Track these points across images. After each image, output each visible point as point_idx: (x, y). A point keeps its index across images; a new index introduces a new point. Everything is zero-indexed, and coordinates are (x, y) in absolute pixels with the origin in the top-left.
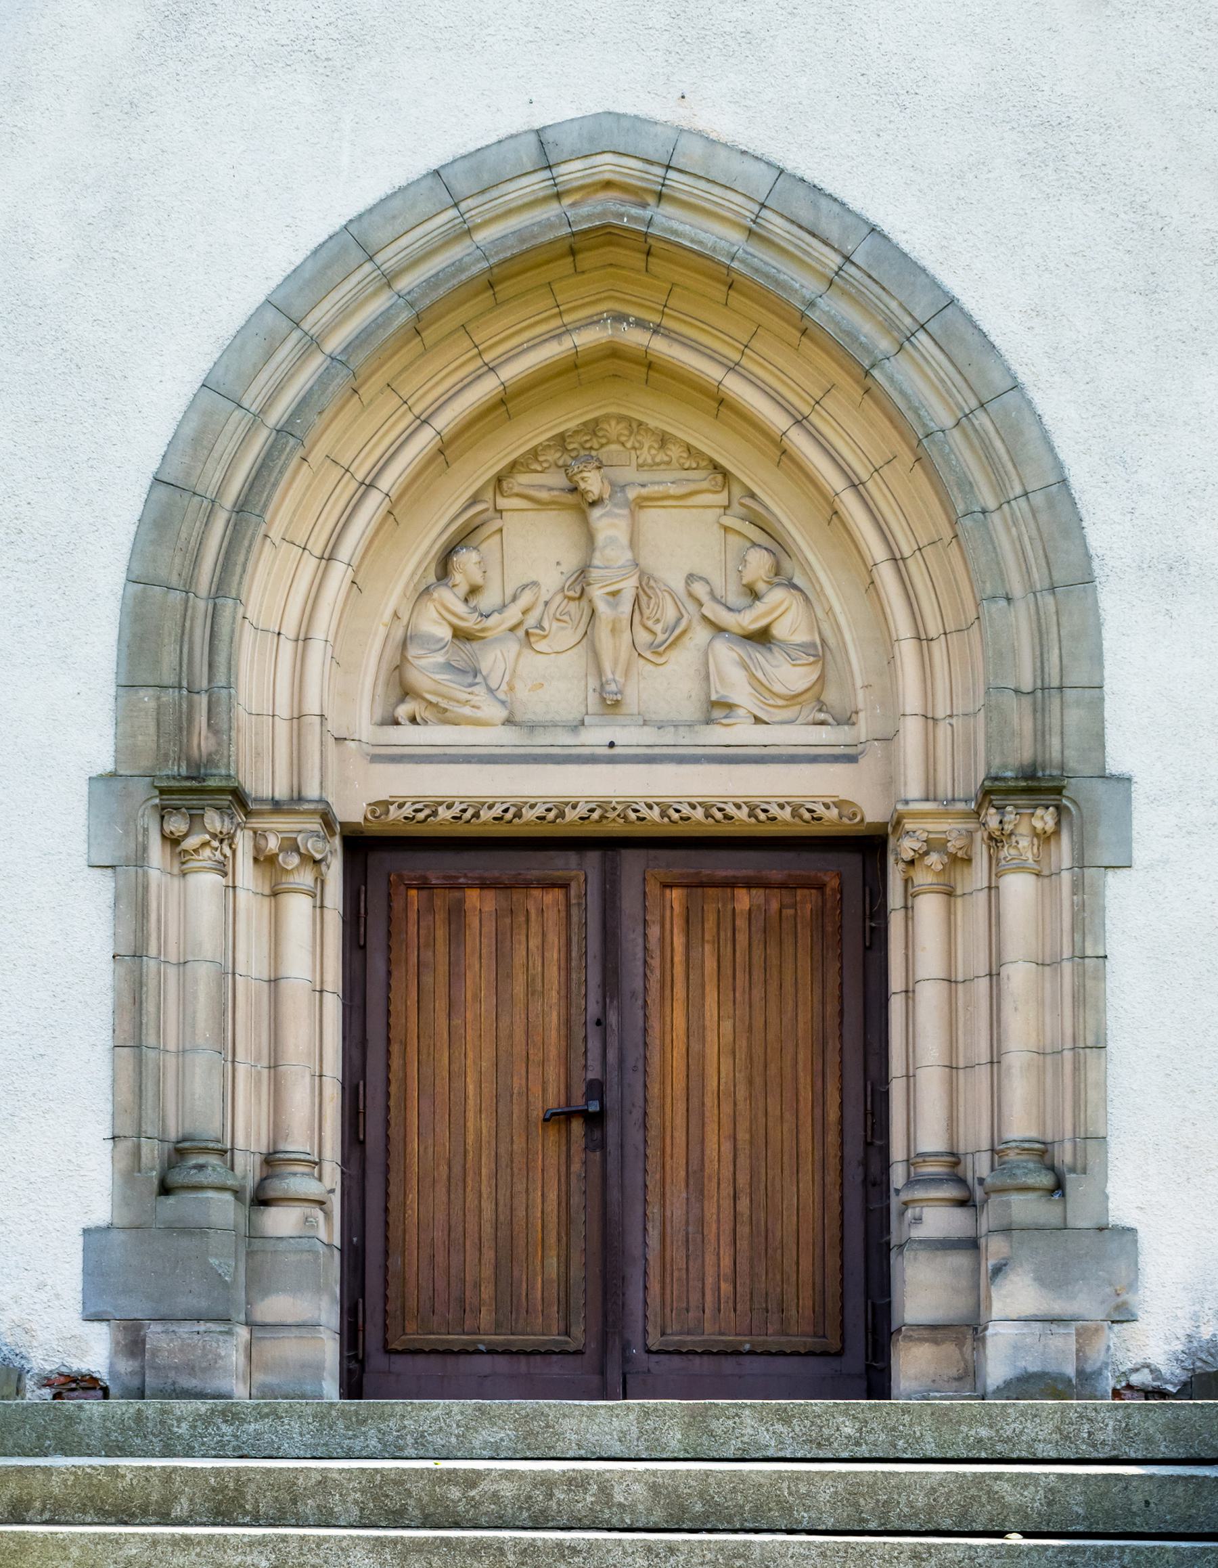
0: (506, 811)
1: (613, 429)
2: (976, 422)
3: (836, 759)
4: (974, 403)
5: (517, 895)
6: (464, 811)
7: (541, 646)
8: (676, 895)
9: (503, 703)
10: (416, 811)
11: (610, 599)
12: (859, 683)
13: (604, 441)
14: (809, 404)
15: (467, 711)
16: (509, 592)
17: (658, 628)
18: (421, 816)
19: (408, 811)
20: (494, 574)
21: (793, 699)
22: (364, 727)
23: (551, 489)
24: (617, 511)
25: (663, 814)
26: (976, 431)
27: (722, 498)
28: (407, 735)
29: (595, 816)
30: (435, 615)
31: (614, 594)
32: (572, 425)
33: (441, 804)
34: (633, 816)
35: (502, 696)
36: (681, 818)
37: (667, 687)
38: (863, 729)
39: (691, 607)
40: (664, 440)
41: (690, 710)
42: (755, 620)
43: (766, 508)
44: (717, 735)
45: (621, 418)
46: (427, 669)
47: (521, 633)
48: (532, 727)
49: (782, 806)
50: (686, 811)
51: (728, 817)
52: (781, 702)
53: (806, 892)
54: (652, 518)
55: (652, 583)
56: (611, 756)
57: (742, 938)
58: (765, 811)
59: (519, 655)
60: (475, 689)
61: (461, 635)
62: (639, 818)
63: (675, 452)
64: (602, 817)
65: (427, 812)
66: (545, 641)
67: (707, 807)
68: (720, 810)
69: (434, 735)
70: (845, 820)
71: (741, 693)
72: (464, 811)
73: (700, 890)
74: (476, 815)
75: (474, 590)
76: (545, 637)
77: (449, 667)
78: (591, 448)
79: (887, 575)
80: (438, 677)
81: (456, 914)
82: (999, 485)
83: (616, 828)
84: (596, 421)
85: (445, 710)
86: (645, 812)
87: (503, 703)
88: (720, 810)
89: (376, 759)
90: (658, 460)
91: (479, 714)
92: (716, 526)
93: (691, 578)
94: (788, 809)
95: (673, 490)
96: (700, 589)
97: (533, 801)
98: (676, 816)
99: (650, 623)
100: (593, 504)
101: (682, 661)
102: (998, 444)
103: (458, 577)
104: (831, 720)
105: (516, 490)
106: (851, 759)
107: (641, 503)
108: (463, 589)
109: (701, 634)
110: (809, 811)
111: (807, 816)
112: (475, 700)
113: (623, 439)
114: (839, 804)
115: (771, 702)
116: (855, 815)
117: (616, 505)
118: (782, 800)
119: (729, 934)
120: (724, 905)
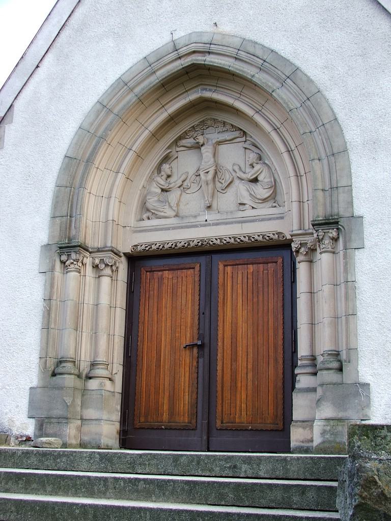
0: (172, 245)
1: (209, 123)
2: (307, 104)
3: (277, 218)
4: (305, 98)
5: (179, 272)
6: (160, 246)
7: (188, 191)
8: (229, 269)
9: (174, 210)
10: (146, 247)
11: (206, 174)
12: (285, 193)
13: (207, 127)
14: (260, 106)
15: (162, 214)
16: (179, 176)
17: (223, 182)
18: (147, 249)
19: (143, 247)
20: (174, 170)
21: (265, 200)
22: (132, 221)
23: (191, 143)
24: (208, 147)
25: (221, 242)
26: (307, 107)
27: (244, 139)
28: (147, 223)
29: (200, 244)
30: (155, 185)
31: (207, 172)
32: (196, 123)
33: (153, 244)
34: (211, 243)
35: (174, 208)
36: (227, 243)
37: (226, 201)
38: (286, 209)
39: (234, 174)
40: (224, 123)
41: (233, 207)
42: (251, 176)
43: (255, 140)
44: (241, 214)
45: (211, 119)
46: (152, 202)
47: (182, 188)
48: (182, 218)
49: (259, 236)
50: (228, 240)
51: (241, 241)
52: (260, 201)
53: (271, 264)
54: (223, 148)
55: (221, 168)
56: (206, 224)
57: (250, 281)
58: (253, 238)
59: (181, 195)
60: (165, 207)
61: (163, 190)
62: (214, 244)
63: (228, 127)
64: (202, 244)
65: (149, 247)
66: (189, 190)
67: (235, 238)
68: (239, 239)
69: (155, 222)
70: (280, 239)
71: (247, 200)
72: (160, 246)
73: (236, 266)
74: (163, 247)
75: (169, 176)
76: (189, 188)
77: (159, 201)
78: (204, 129)
79: (286, 156)
80: (154, 204)
81: (161, 279)
82: (315, 123)
83: (207, 248)
84: (203, 121)
85: (157, 214)
86: (215, 241)
87: (174, 210)
88: (239, 239)
89: (135, 232)
90: (224, 130)
91: (166, 215)
92: (242, 148)
93: (234, 164)
94: (261, 237)
95: (228, 138)
96: (236, 168)
97: (180, 241)
98: (225, 242)
99: (220, 180)
100: (202, 145)
101: (231, 191)
102: (314, 110)
103: (163, 173)
104: (277, 206)
105: (181, 145)
106: (282, 218)
107: (219, 143)
108: (165, 176)
109: (237, 182)
110: (268, 236)
111: (267, 238)
112: (165, 210)
113: (213, 125)
114: (279, 233)
115: (257, 201)
116: (284, 237)
117: (208, 145)
118: (259, 234)
119: (246, 280)
120: (244, 271)
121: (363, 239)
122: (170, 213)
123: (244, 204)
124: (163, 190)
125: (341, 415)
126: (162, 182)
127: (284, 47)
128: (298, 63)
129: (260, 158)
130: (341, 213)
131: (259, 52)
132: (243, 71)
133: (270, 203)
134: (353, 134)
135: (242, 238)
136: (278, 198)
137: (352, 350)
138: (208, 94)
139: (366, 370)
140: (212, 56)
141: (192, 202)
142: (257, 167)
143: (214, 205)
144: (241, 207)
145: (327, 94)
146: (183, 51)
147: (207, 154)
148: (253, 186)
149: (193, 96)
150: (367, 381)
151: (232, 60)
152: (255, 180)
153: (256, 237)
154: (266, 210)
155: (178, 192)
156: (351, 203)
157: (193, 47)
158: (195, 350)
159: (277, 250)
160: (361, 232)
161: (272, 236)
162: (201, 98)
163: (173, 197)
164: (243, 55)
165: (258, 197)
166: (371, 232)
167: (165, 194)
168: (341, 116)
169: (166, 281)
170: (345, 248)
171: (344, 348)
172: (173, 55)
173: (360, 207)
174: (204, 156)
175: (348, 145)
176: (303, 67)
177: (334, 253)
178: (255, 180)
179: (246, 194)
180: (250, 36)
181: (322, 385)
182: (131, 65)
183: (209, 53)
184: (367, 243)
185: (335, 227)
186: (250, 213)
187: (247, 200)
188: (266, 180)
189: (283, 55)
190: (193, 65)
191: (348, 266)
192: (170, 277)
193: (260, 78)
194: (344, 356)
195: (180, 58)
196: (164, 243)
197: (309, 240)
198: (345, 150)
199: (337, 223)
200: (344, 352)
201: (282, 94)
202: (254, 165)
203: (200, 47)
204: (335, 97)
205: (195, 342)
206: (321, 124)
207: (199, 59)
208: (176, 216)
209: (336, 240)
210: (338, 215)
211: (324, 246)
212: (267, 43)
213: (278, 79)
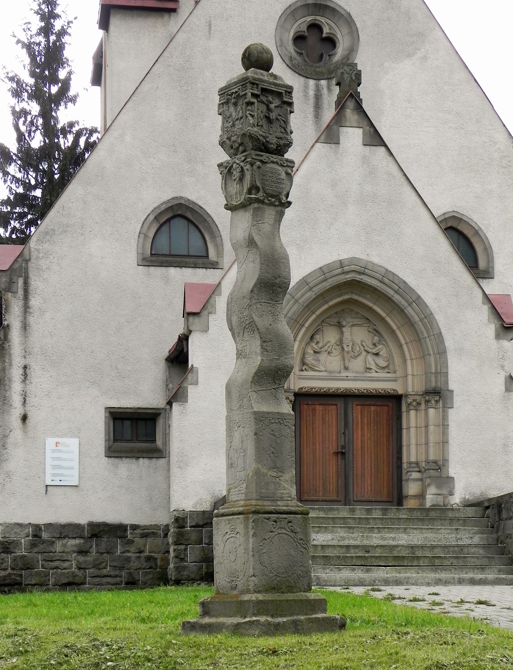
5: (327, 406)
8: (359, 407)
15: (318, 369)
17: (355, 352)
21: (383, 368)
28: (305, 373)
31: (348, 346)
39: (362, 348)
40: (357, 313)
41: (362, 369)
46: (310, 359)
48: (331, 372)
50: (363, 390)
54: (355, 328)
56: (347, 379)
57: (372, 416)
71: (373, 367)
77: (314, 359)
81: (314, 410)
83: (349, 393)
93: (362, 341)
95: (359, 323)
96: (364, 344)
103: (315, 341)
107: (353, 325)
108: (315, 343)
109: (364, 353)
114: (394, 390)
121: (452, 403)
122: (322, 368)
123: (371, 369)
124: (315, 352)
125: (439, 492)
126: (316, 347)
127: (412, 281)
128: (420, 293)
129: (380, 341)
130: (442, 387)
131: (397, 282)
132: (386, 292)
133: (386, 370)
134: (449, 343)
135: (372, 391)
136: (391, 366)
137: (446, 461)
138: (356, 297)
139: (453, 471)
140: (365, 276)
141: (332, 362)
142: (380, 347)
143: (350, 367)
144: (368, 370)
145: (435, 316)
146: (346, 269)
147: (347, 333)
148: (375, 358)
149: (346, 297)
150: (452, 476)
151: (378, 282)
152: (377, 354)
153: (380, 391)
154: (383, 375)
155: (326, 354)
156: (447, 382)
157: (353, 267)
158: (340, 455)
159: (394, 400)
160: (452, 399)
161: (390, 391)
162: (351, 298)
163: (323, 357)
164: (386, 280)
165: (380, 365)
166: (457, 400)
167: (317, 355)
168: (443, 331)
169: (317, 411)
170: (444, 407)
171: (441, 459)
172: (339, 271)
173: (452, 386)
174: (345, 334)
175: (447, 349)
176: (423, 296)
177: (435, 408)
178: (377, 354)
179: (372, 363)
180: (390, 268)
181: (430, 477)
182: (310, 271)
183: (363, 274)
184: (455, 405)
185: (437, 394)
186: (374, 375)
187: (373, 367)
188: (384, 355)
189: (411, 285)
190: (353, 280)
191: (445, 417)
192: (321, 409)
193: (397, 298)
194: (441, 463)
195: (344, 273)
196: (321, 389)
197: (418, 398)
198: (445, 352)
199: (440, 393)
200: (441, 461)
201: (409, 311)
202: (377, 344)
203: (358, 268)
204: (440, 318)
205: (340, 450)
206: (432, 334)
207: (358, 277)
208: (325, 371)
209: (437, 402)
210: (440, 388)
211: (430, 404)
212: (401, 275)
213: (407, 301)
